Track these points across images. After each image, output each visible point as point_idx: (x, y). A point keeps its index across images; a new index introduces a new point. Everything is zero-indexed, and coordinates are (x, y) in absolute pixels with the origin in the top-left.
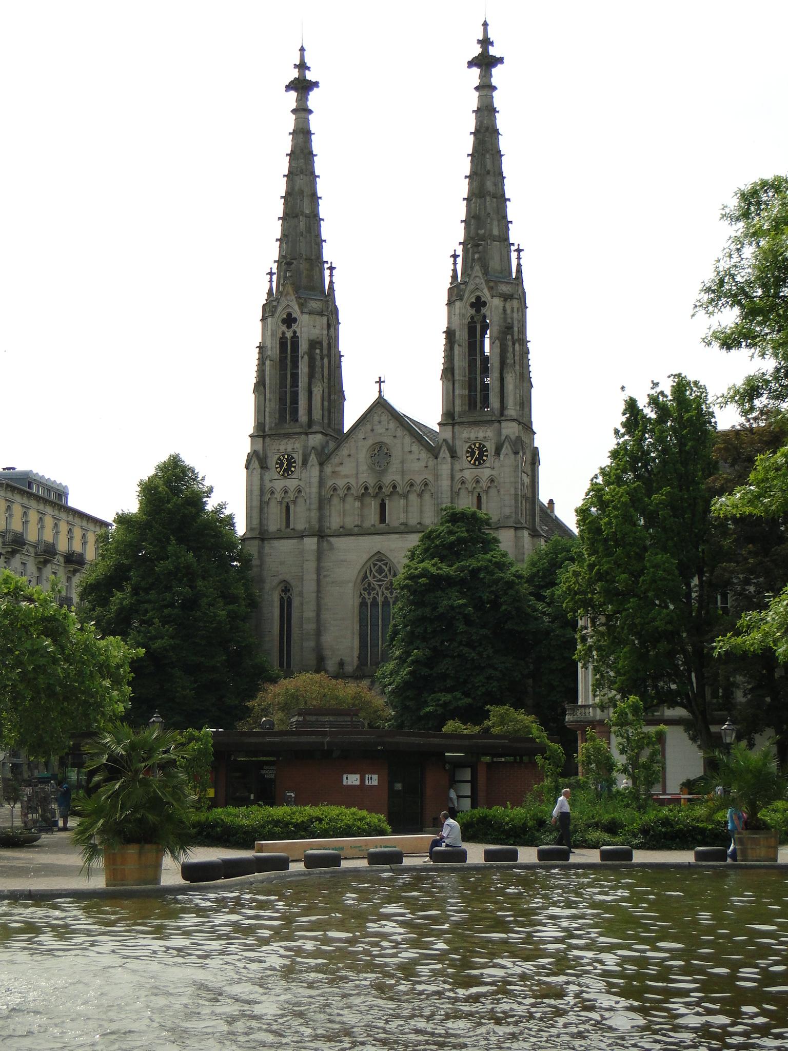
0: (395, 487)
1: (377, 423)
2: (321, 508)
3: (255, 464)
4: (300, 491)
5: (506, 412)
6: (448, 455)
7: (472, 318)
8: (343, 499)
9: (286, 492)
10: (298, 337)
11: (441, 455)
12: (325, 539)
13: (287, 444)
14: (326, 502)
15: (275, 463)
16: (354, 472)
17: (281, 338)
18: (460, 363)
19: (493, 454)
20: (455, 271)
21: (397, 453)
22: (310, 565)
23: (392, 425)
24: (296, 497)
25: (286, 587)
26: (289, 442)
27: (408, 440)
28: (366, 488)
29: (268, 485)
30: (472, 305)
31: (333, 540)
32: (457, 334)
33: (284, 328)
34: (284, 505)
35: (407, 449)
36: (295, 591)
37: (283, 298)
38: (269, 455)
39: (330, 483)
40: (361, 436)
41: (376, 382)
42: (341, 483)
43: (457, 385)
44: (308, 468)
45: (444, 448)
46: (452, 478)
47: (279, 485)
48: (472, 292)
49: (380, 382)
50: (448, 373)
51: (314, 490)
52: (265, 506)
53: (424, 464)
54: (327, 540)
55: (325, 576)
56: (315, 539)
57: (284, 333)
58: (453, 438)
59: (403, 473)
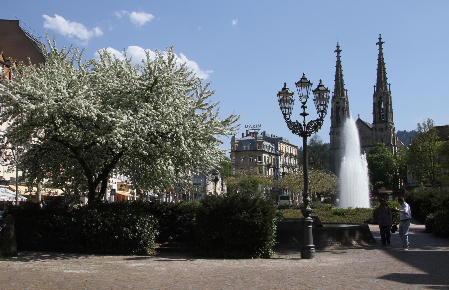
3: (332, 133)
7: (379, 100)
18: (377, 110)
20: (375, 90)
30: (379, 98)
32: (376, 104)
33: (336, 104)
43: (376, 115)
46: (376, 135)
49: (359, 115)
50: (374, 113)
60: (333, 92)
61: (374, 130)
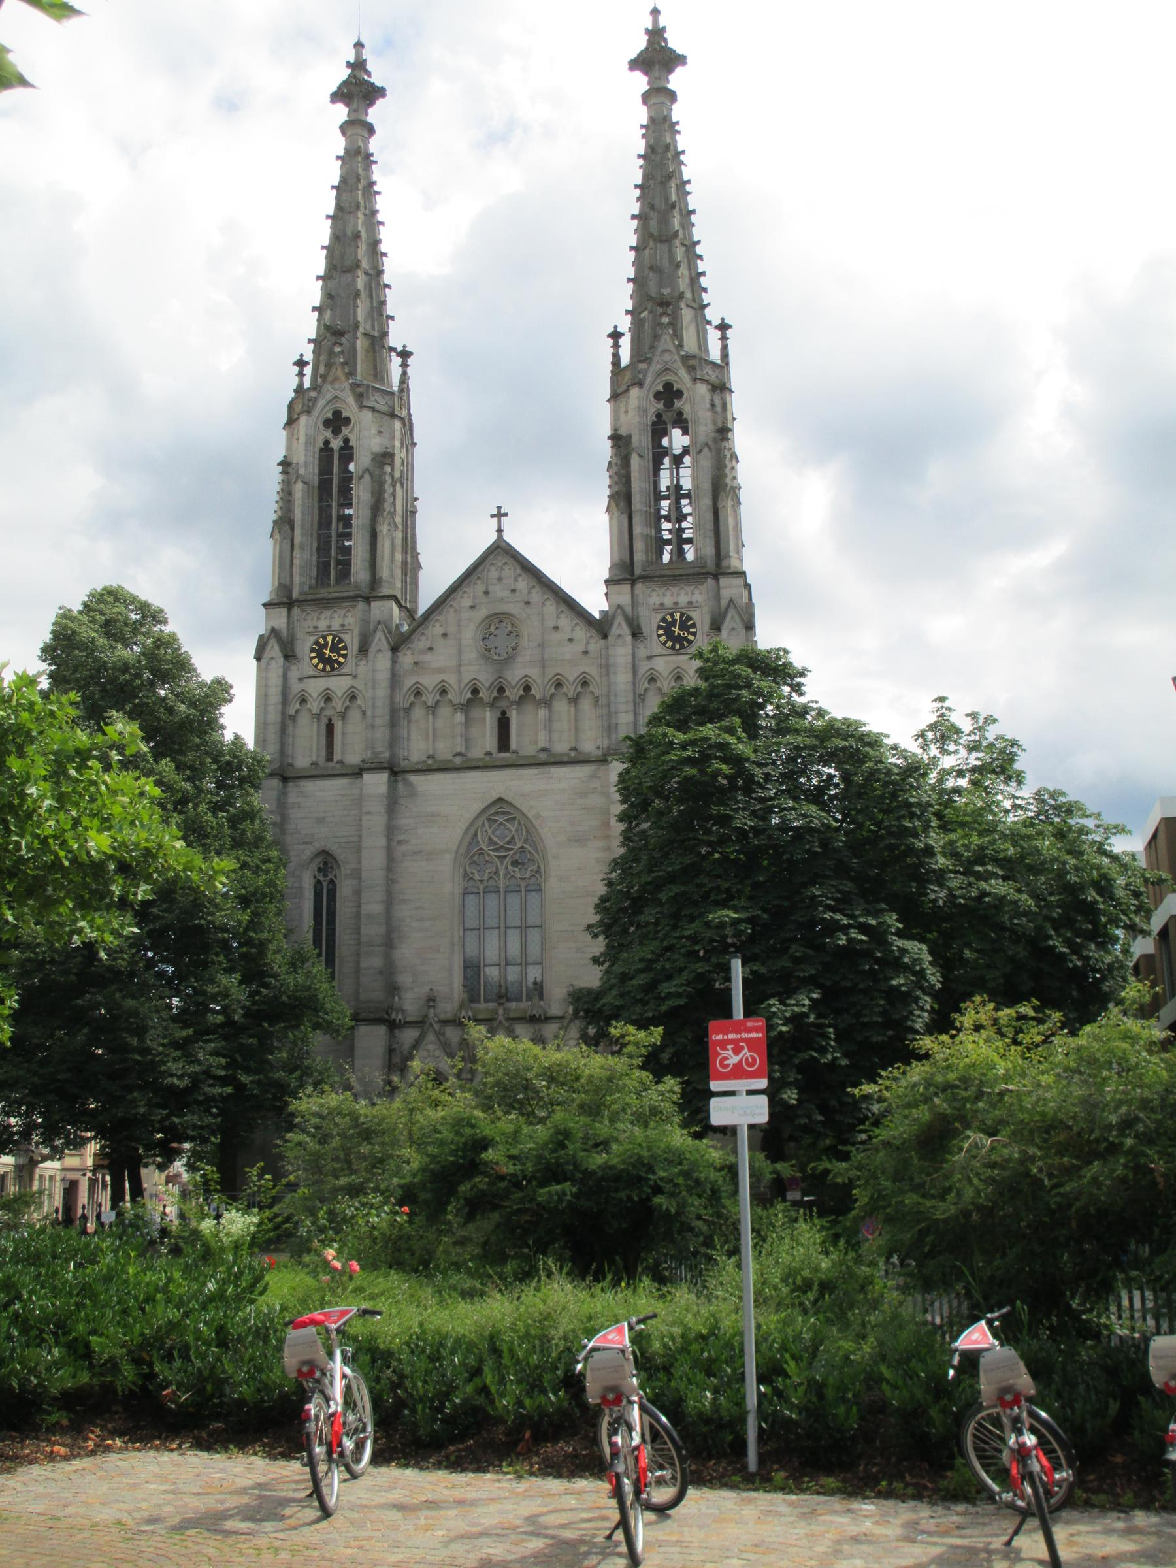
0: (527, 688)
1: (495, 581)
2: (393, 724)
3: (274, 650)
4: (353, 698)
5: (724, 563)
6: (626, 631)
7: (659, 416)
8: (433, 709)
9: (328, 699)
10: (352, 448)
11: (614, 631)
12: (400, 778)
13: (331, 618)
14: (402, 714)
15: (308, 649)
16: (454, 663)
17: (321, 450)
19: (707, 628)
21: (530, 633)
22: (376, 822)
23: (523, 584)
24: (347, 708)
25: (325, 863)
26: (336, 615)
27: (551, 608)
28: (475, 691)
29: (296, 687)
30: (658, 396)
31: (413, 778)
32: (635, 441)
33: (328, 434)
34: (324, 721)
35: (550, 623)
36: (345, 870)
37: (327, 387)
38: (300, 635)
39: (409, 682)
40: (466, 602)
41: (493, 516)
42: (429, 681)
43: (637, 520)
44: (371, 654)
45: (620, 619)
46: (635, 670)
47: (315, 687)
48: (659, 375)
49: (500, 515)
51: (382, 691)
52: (288, 721)
53: (582, 648)
54: (404, 780)
55: (400, 842)
56: (384, 776)
57: (327, 442)
58: (634, 603)
59: (543, 664)
60: (301, 363)
61: (620, 628)
